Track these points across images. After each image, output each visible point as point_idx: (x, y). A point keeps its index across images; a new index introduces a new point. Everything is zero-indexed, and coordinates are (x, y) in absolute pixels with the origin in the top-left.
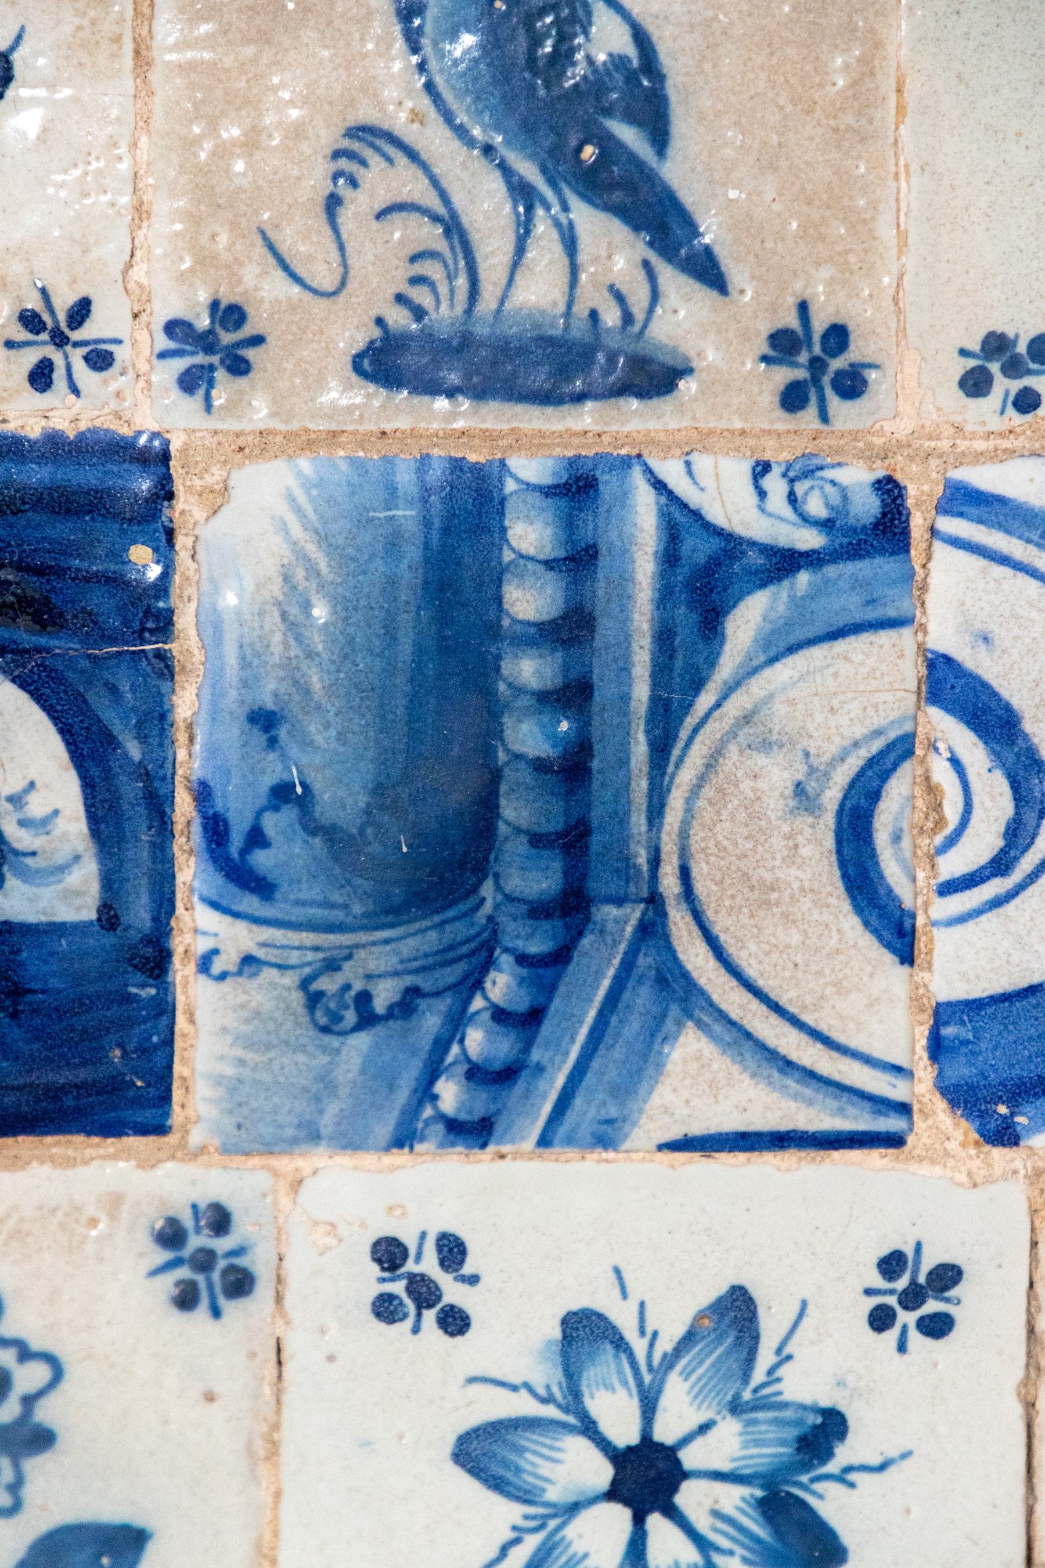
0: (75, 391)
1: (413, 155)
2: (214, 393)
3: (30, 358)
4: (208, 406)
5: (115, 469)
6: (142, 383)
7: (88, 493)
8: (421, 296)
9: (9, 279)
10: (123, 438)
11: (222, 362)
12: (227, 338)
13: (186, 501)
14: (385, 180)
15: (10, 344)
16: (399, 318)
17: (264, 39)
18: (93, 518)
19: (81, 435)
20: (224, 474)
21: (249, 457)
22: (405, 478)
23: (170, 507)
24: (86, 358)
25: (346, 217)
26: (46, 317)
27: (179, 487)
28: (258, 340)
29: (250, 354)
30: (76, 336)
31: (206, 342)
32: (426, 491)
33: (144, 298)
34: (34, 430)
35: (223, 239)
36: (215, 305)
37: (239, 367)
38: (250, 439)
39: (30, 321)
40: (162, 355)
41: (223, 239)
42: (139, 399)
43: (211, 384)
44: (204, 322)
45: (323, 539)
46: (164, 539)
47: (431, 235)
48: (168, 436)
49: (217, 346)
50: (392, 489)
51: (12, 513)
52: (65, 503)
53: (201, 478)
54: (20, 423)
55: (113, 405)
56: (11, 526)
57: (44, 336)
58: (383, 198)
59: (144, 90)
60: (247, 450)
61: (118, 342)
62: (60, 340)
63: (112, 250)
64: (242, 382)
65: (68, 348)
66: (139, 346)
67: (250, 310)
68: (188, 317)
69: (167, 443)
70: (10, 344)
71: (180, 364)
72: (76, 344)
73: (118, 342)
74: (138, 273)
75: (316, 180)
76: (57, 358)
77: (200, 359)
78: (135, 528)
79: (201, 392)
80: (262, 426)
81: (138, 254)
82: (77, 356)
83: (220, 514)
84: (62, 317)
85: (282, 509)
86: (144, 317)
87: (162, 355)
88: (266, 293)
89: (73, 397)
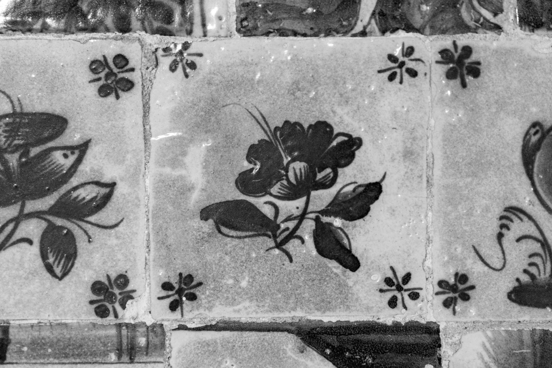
0: (405, 307)
1: (530, 218)
2: (456, 307)
3: (389, 295)
4: (454, 312)
5: (419, 336)
6: (429, 304)
7: (410, 345)
8: (533, 270)
9: (381, 267)
10: (422, 324)
11: (460, 296)
12: (461, 287)
13: (446, 348)
14: (520, 227)
15: (381, 291)
16: (525, 278)
17: (474, 175)
18: (411, 355)
19: (407, 323)
20: (460, 337)
21: (469, 331)
22: (527, 338)
23: (440, 350)
24: (409, 295)
25: (505, 241)
26: (394, 280)
27: (443, 342)
28: (472, 287)
29: (470, 293)
30: (405, 287)
31: (453, 288)
32: (534, 343)
33: (430, 273)
34: (389, 322)
35: (459, 250)
36: (456, 274)
37: (466, 298)
38: (469, 324)
39: (388, 281)
40: (437, 294)
41: (459, 250)
42: (428, 309)
43: (455, 305)
44: (452, 281)
45: (496, 361)
46: (438, 362)
47: (536, 247)
48: (439, 323)
49: (457, 290)
50: (522, 342)
51: (382, 353)
52: (401, 349)
53: (451, 339)
54: (384, 319)
55: (419, 312)
56: (382, 358)
57: (394, 288)
58: (519, 234)
59: (431, 195)
60: (468, 328)
61: (421, 289)
62: (399, 289)
63: (418, 256)
64: (467, 303)
65: (403, 292)
66: (429, 290)
67: (470, 277)
68: (447, 279)
69: (439, 326)
70: (381, 291)
71: (444, 297)
72: (406, 290)
73: (421, 289)
74: (428, 263)
75: (494, 227)
76: (399, 296)
77: (451, 295)
78: (427, 358)
79: (452, 307)
80: (474, 319)
81: (428, 256)
82: (406, 295)
83: (458, 353)
84: (400, 280)
85: (481, 350)
86: (430, 279)
87: (437, 294)
88: (475, 270)
89: (404, 310)
